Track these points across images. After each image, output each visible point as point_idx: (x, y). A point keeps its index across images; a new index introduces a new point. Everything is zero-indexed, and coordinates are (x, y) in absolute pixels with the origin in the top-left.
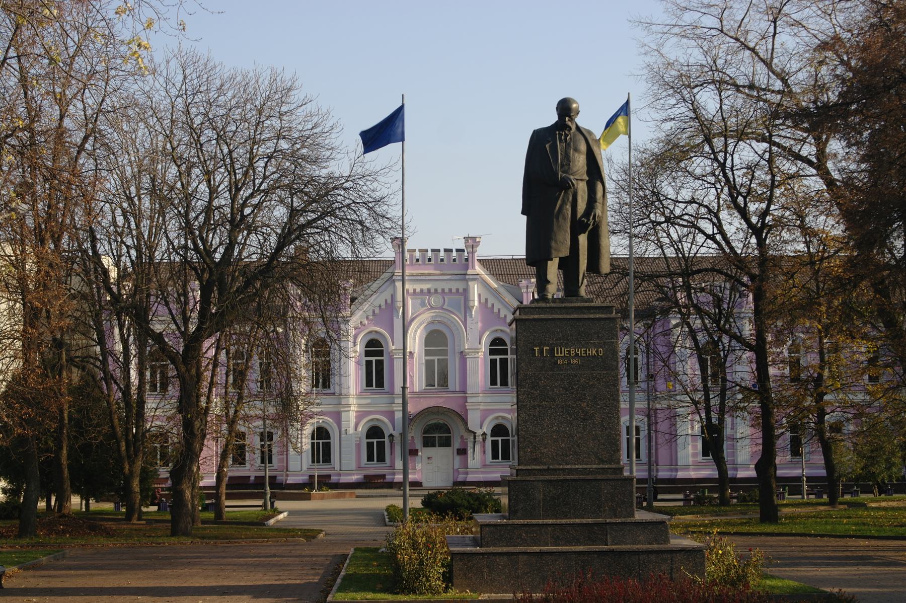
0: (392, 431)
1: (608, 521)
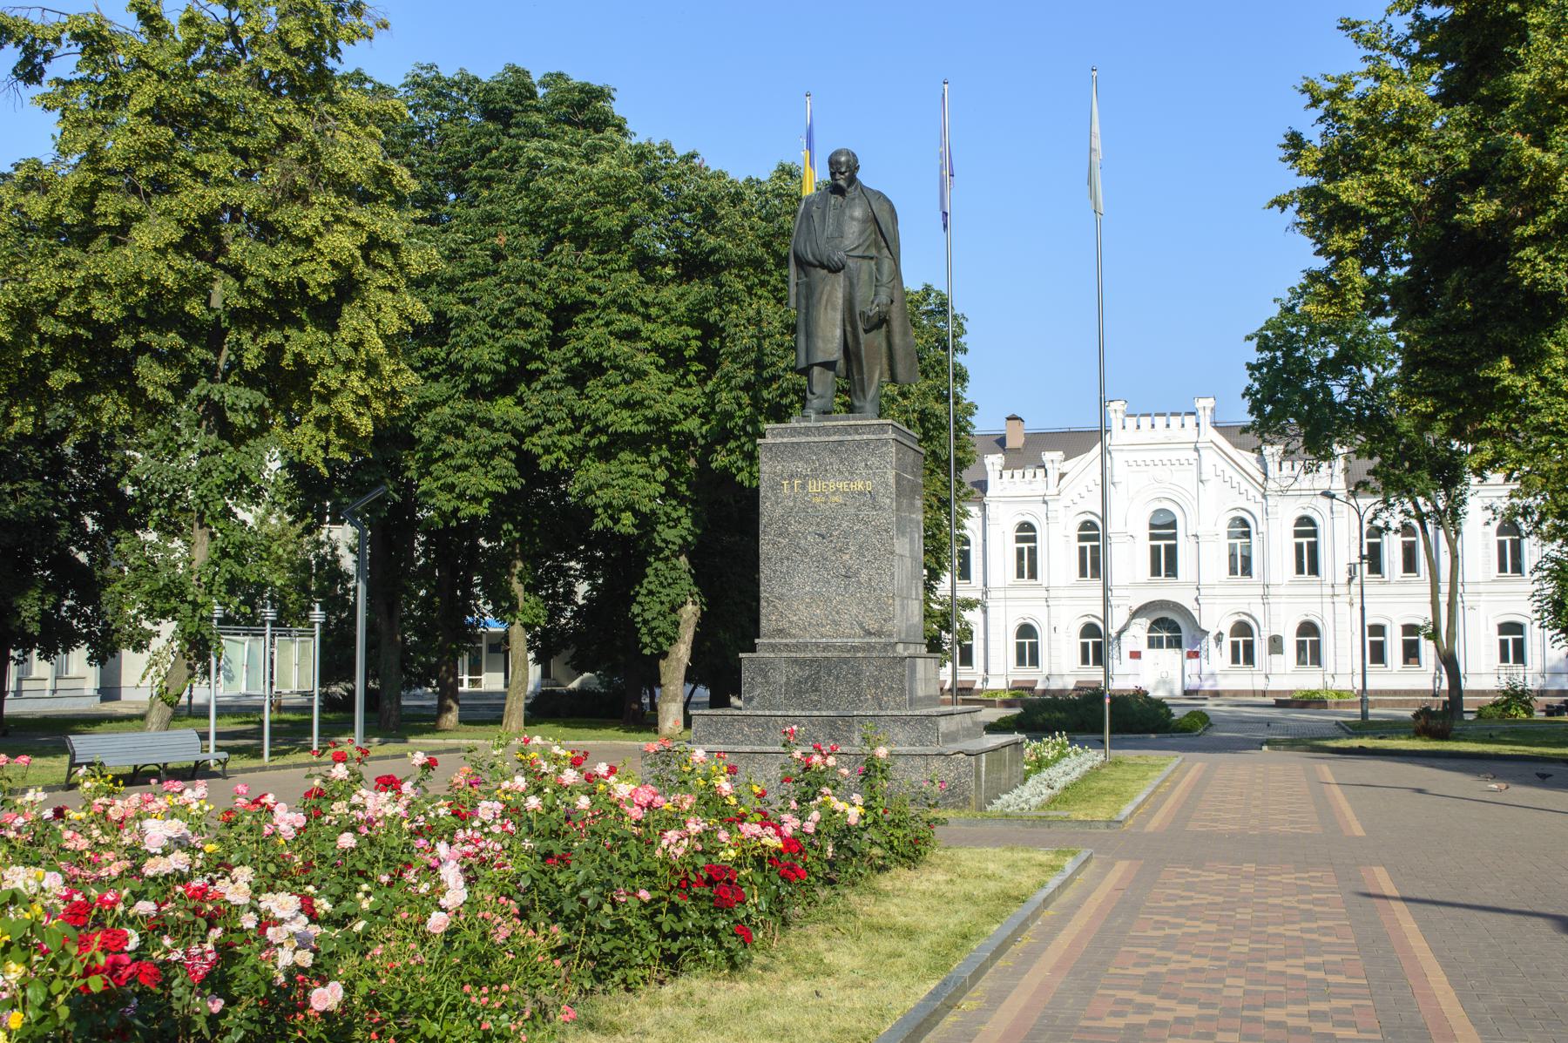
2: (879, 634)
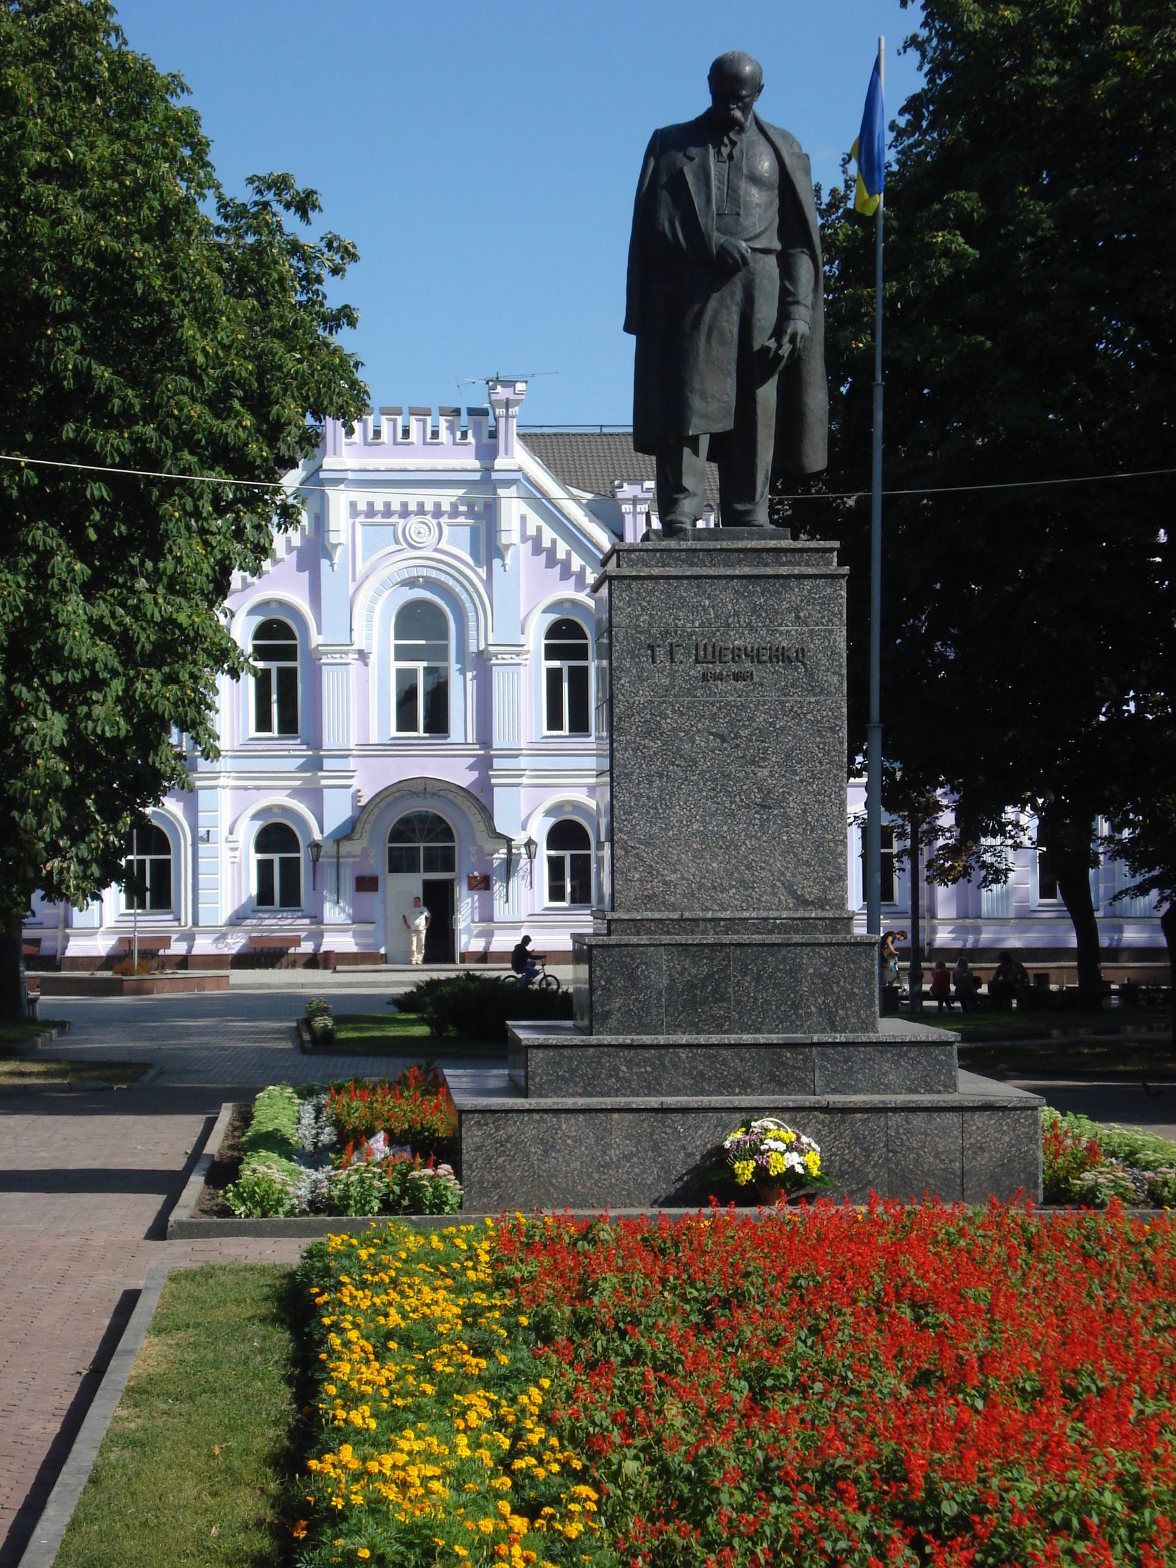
0: (317, 836)
1: (816, 1039)
2: (821, 903)
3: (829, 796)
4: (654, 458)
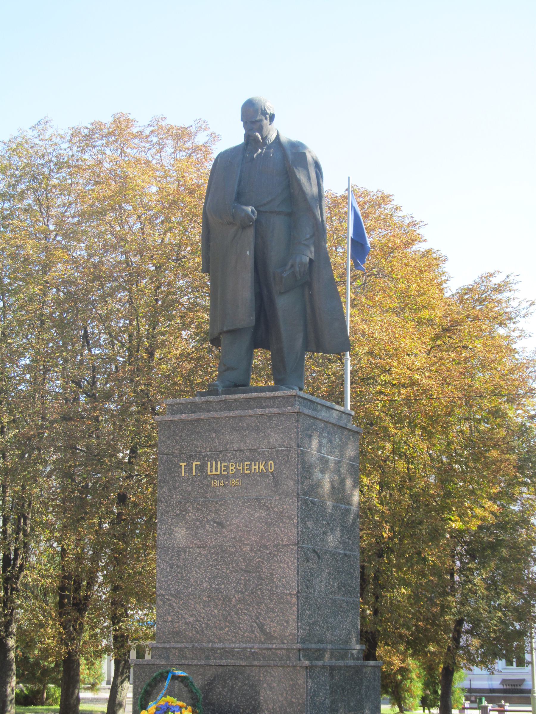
3: (287, 564)
4: (269, 354)
